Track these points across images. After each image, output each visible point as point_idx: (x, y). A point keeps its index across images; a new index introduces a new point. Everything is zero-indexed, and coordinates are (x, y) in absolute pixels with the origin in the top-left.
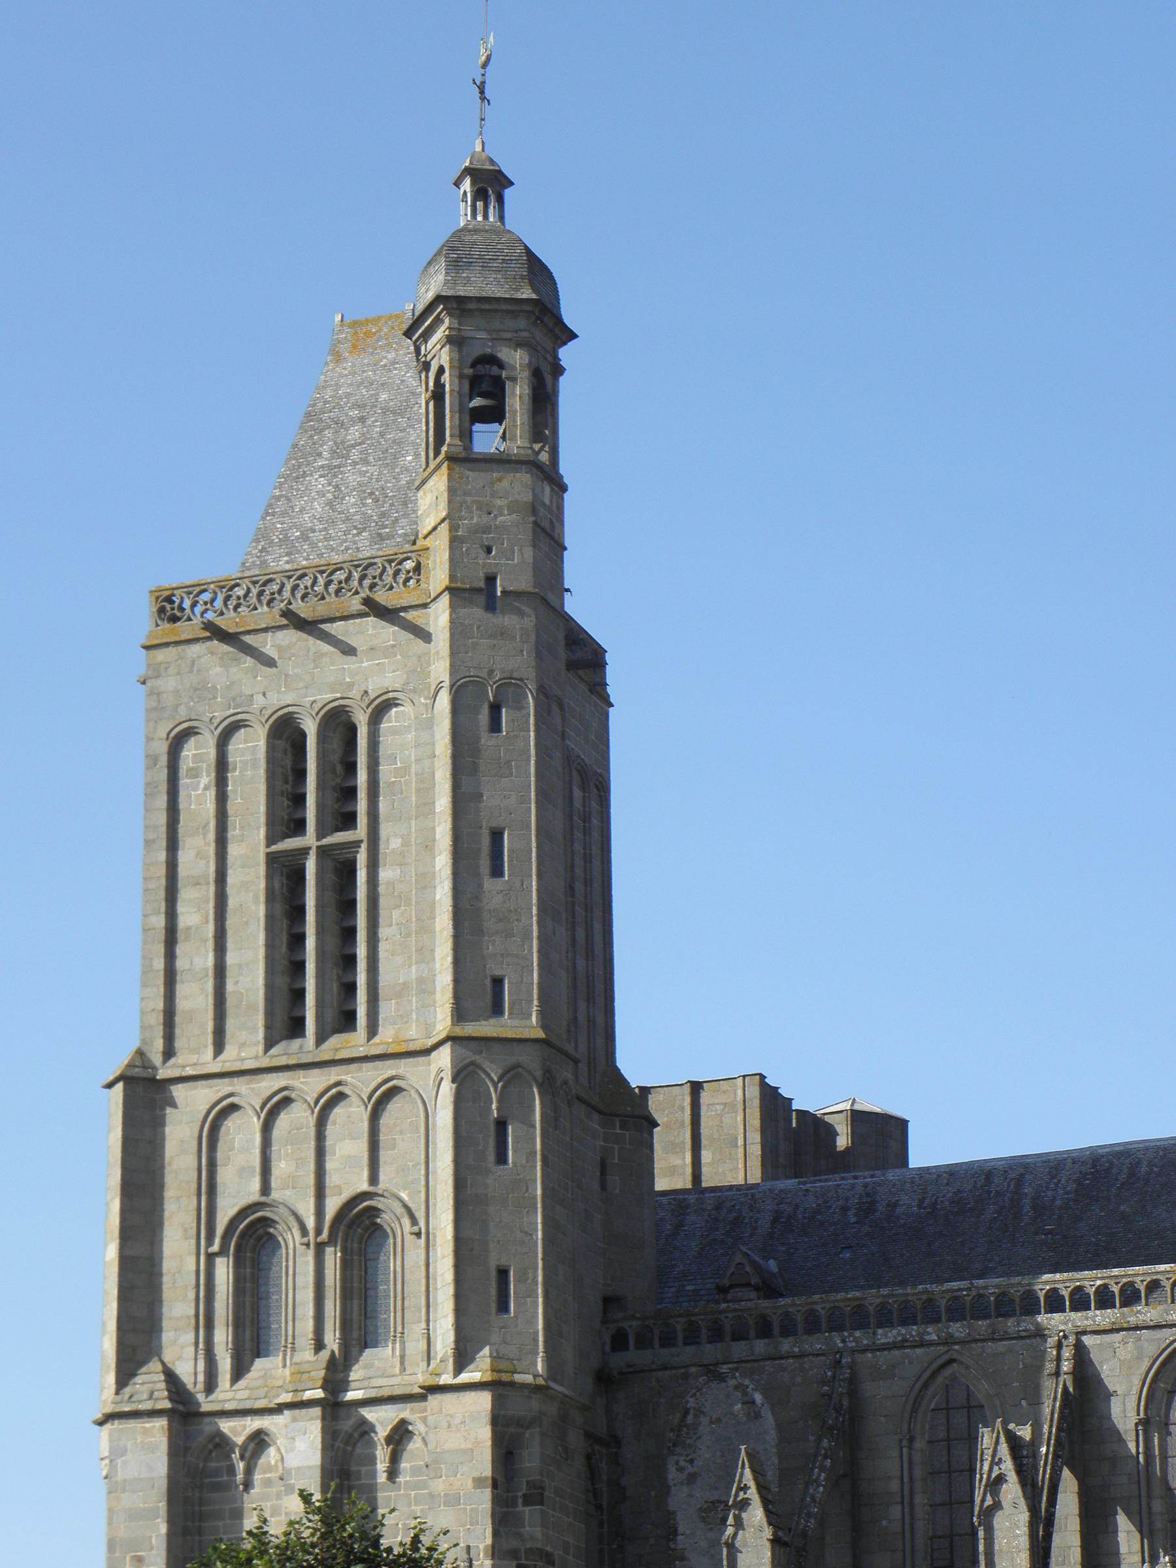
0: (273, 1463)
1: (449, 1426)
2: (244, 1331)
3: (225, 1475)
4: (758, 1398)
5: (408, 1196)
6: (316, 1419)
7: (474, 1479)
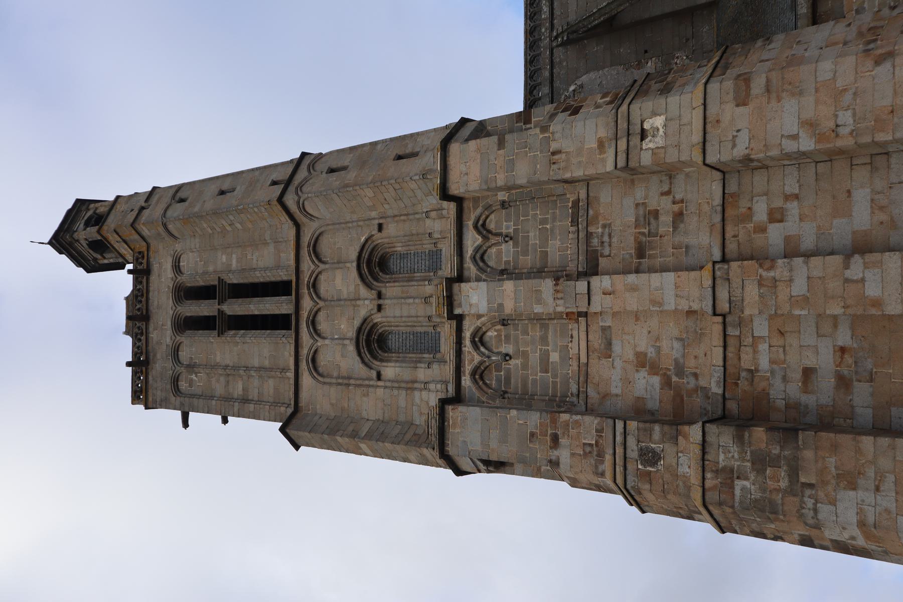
0: (496, 333)
1: (467, 174)
2: (424, 358)
4: (572, 88)
5: (363, 236)
6: (460, 286)
7: (498, 150)
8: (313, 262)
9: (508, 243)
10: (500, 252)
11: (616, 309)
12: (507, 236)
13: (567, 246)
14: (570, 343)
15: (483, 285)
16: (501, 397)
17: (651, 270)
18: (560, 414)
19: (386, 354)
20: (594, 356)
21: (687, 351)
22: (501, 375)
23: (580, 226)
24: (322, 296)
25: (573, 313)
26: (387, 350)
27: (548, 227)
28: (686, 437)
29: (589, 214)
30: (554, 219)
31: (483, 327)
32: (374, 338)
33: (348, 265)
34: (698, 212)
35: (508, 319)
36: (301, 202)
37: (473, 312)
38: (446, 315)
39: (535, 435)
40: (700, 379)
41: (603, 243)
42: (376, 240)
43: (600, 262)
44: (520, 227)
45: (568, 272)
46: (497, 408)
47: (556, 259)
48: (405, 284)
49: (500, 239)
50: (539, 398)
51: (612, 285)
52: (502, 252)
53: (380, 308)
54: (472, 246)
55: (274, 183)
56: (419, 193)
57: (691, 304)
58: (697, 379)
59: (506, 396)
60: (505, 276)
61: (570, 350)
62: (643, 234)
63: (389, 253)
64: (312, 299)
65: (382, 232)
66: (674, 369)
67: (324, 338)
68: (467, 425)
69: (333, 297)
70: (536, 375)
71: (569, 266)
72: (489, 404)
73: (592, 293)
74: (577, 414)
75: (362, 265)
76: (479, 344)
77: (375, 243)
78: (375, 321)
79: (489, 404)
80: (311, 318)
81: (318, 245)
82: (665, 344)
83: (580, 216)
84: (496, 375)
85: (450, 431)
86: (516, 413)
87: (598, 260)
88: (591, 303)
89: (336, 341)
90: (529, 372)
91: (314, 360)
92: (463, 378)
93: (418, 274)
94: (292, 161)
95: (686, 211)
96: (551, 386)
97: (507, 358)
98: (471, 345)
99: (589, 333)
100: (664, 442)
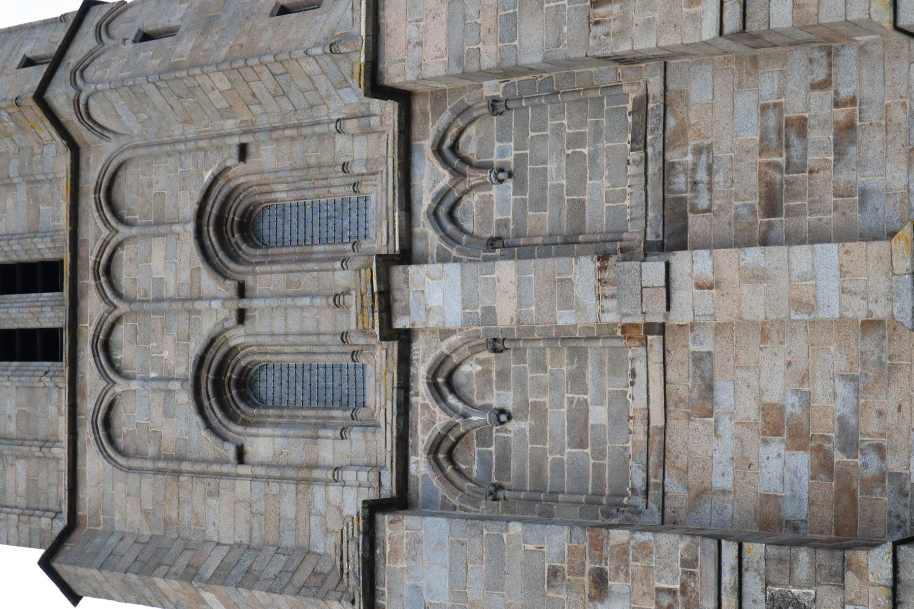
0: (479, 368)
1: (420, 44)
2: (332, 418)
3: (490, 449)
5: (207, 170)
6: (406, 272)
8: (106, 222)
9: (505, 184)
10: (486, 204)
11: (723, 317)
12: (501, 170)
13: (625, 191)
14: (630, 387)
15: (453, 269)
16: (490, 498)
17: (793, 239)
18: (611, 531)
19: (255, 411)
20: (677, 412)
21: (862, 401)
22: (491, 453)
23: (650, 150)
24: (123, 291)
25: (636, 326)
26: (257, 401)
27: (585, 151)
28: (861, 573)
29: (668, 127)
30: (597, 136)
31: (453, 355)
32: (230, 377)
33: (177, 228)
34: (883, 122)
35: (504, 340)
36: (82, 102)
37: (432, 324)
38: (377, 330)
39: (558, 574)
40: (888, 457)
41: (695, 183)
42: (235, 178)
43: (690, 221)
44: (528, 152)
45: (624, 244)
46: (483, 519)
47: (601, 217)
48: (294, 267)
49: (487, 176)
50: (568, 497)
51: (715, 268)
52: (493, 203)
53: (242, 316)
54: (431, 190)
55: (28, 62)
56: (323, 84)
57: (872, 306)
58: (883, 458)
59: (500, 494)
60: (498, 251)
61: (630, 400)
62: (776, 166)
63: (261, 204)
64: (104, 297)
65: (248, 161)
66: (839, 437)
67: (128, 378)
68: (421, 553)
69: (146, 294)
70: (562, 452)
71: (627, 231)
72: (466, 510)
73: (674, 285)
74: (645, 530)
75: (205, 228)
76: (445, 390)
77: (232, 184)
78: (232, 343)
79: (466, 510)
80: (101, 337)
81: (115, 188)
82: (820, 389)
83: (649, 129)
84: (479, 451)
85: (387, 565)
86: (520, 529)
87: (686, 218)
88: (672, 305)
89: (154, 385)
90: (548, 446)
91: (107, 423)
92: (412, 459)
93: (321, 248)
94: (63, 18)
95: (861, 120)
96: (591, 474)
97: (503, 418)
98: (429, 392)
99: (668, 367)
100: (817, 584)
